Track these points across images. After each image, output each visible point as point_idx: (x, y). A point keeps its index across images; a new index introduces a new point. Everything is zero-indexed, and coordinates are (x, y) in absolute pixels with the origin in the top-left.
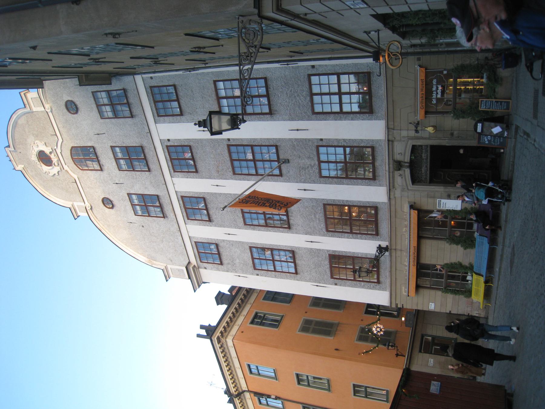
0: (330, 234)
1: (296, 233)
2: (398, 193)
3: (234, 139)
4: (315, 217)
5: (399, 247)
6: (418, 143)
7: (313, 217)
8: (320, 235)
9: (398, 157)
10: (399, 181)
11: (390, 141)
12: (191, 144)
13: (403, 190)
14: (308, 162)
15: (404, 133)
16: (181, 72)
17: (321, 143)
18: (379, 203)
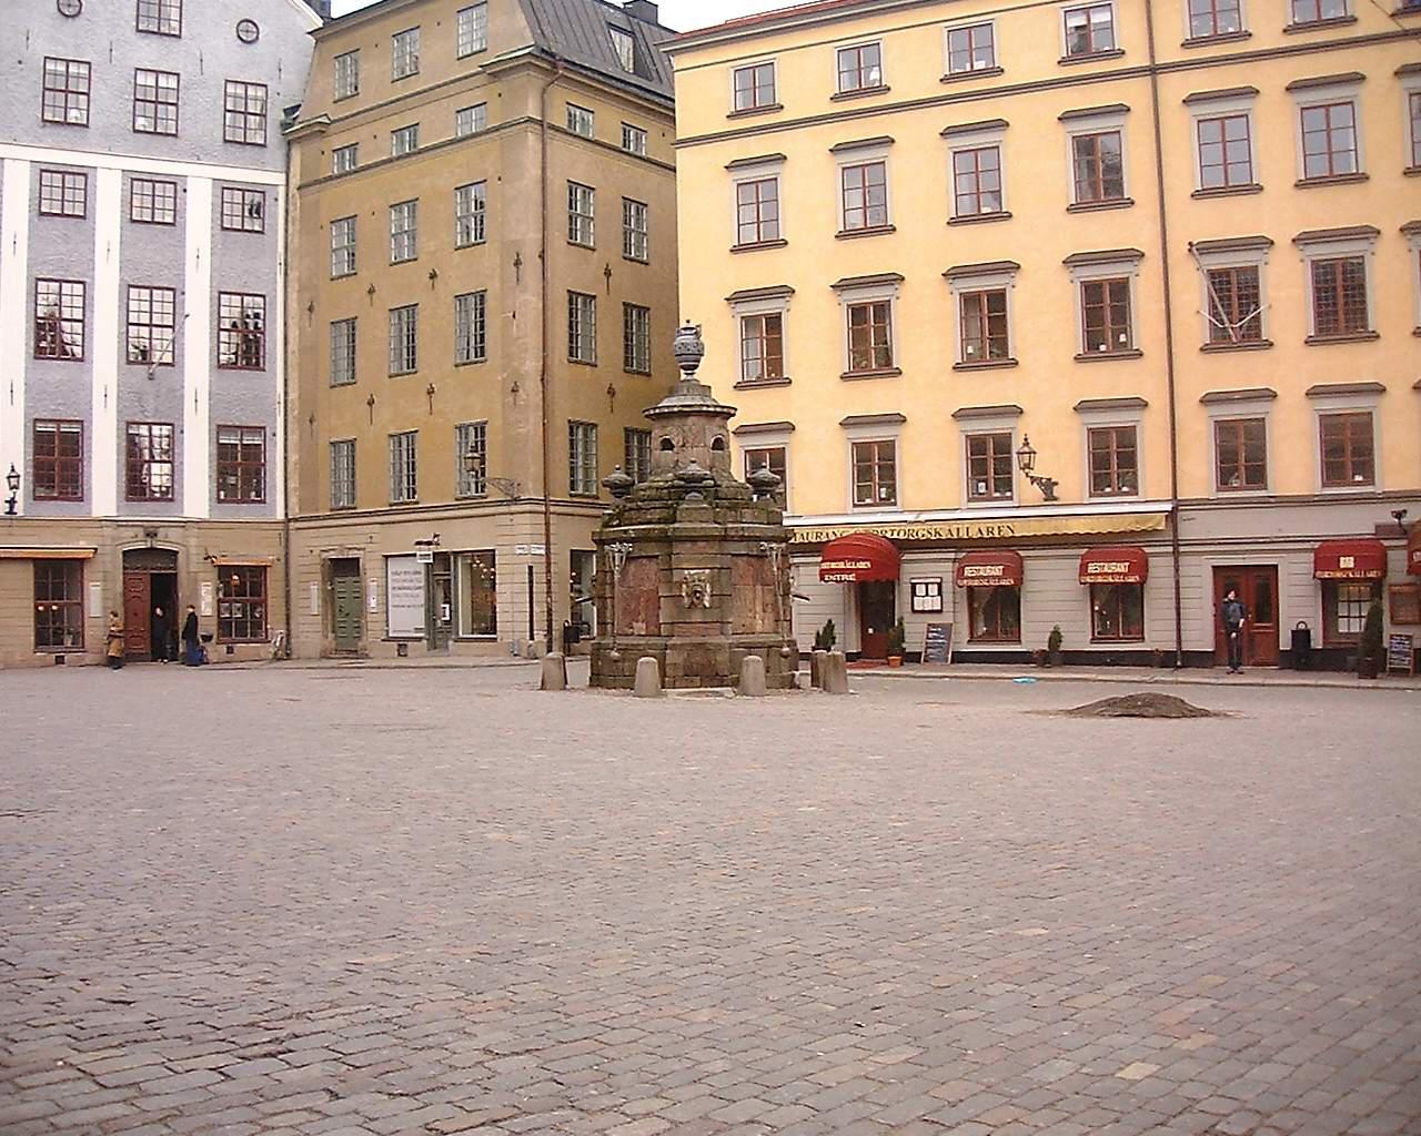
0: (30, 425)
1: (27, 368)
2: (108, 531)
3: (183, 302)
4: (60, 404)
5: (15, 531)
6: (180, 557)
7: (60, 401)
8: (26, 407)
9: (161, 532)
10: (130, 532)
11: (185, 524)
12: (178, 229)
13: (113, 539)
14: (150, 407)
15: (193, 541)
16: (281, 249)
17: (177, 431)
18: (90, 504)
